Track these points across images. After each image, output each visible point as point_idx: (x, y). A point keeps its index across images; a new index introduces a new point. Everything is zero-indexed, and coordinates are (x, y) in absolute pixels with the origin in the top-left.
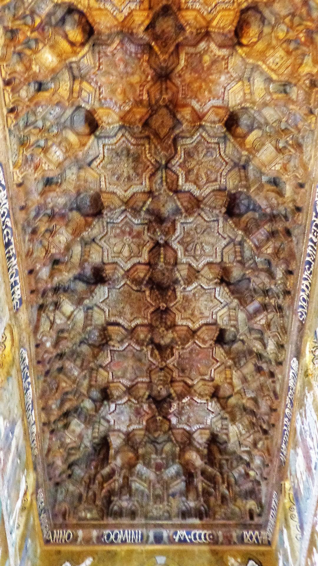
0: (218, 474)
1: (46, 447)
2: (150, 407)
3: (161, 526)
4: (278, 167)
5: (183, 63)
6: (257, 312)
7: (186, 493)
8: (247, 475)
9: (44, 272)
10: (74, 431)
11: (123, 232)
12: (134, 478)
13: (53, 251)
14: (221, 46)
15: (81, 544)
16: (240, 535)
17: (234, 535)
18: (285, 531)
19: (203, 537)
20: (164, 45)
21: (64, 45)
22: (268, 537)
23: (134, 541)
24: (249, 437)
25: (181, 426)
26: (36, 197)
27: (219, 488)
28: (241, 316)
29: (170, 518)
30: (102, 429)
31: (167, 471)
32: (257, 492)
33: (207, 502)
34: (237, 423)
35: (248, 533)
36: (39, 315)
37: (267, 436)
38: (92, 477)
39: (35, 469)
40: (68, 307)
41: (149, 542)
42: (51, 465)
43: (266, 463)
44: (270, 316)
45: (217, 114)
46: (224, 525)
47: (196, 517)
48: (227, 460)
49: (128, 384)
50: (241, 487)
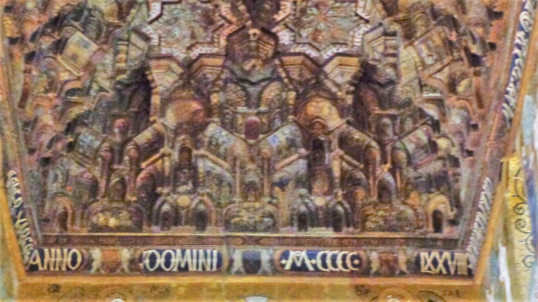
0: (374, 144)
1: (19, 87)
2: (234, 9)
3: (257, 241)
8: (433, 147)
10: (74, 57)
12: (202, 152)
15: (98, 274)
16: (413, 260)
17: (402, 258)
18: (503, 250)
19: (339, 262)
22: (468, 263)
23: (204, 268)
24: (440, 71)
25: (299, 49)
27: (374, 170)
29: (274, 227)
30: (134, 53)
31: (270, 138)
32: (451, 179)
33: (350, 197)
34: (416, 43)
35: (430, 254)
37: (477, 68)
38: (116, 148)
41: (234, 270)
43: (472, 123)
46: (382, 241)
47: (327, 226)
48: (393, 117)
50: (420, 171)
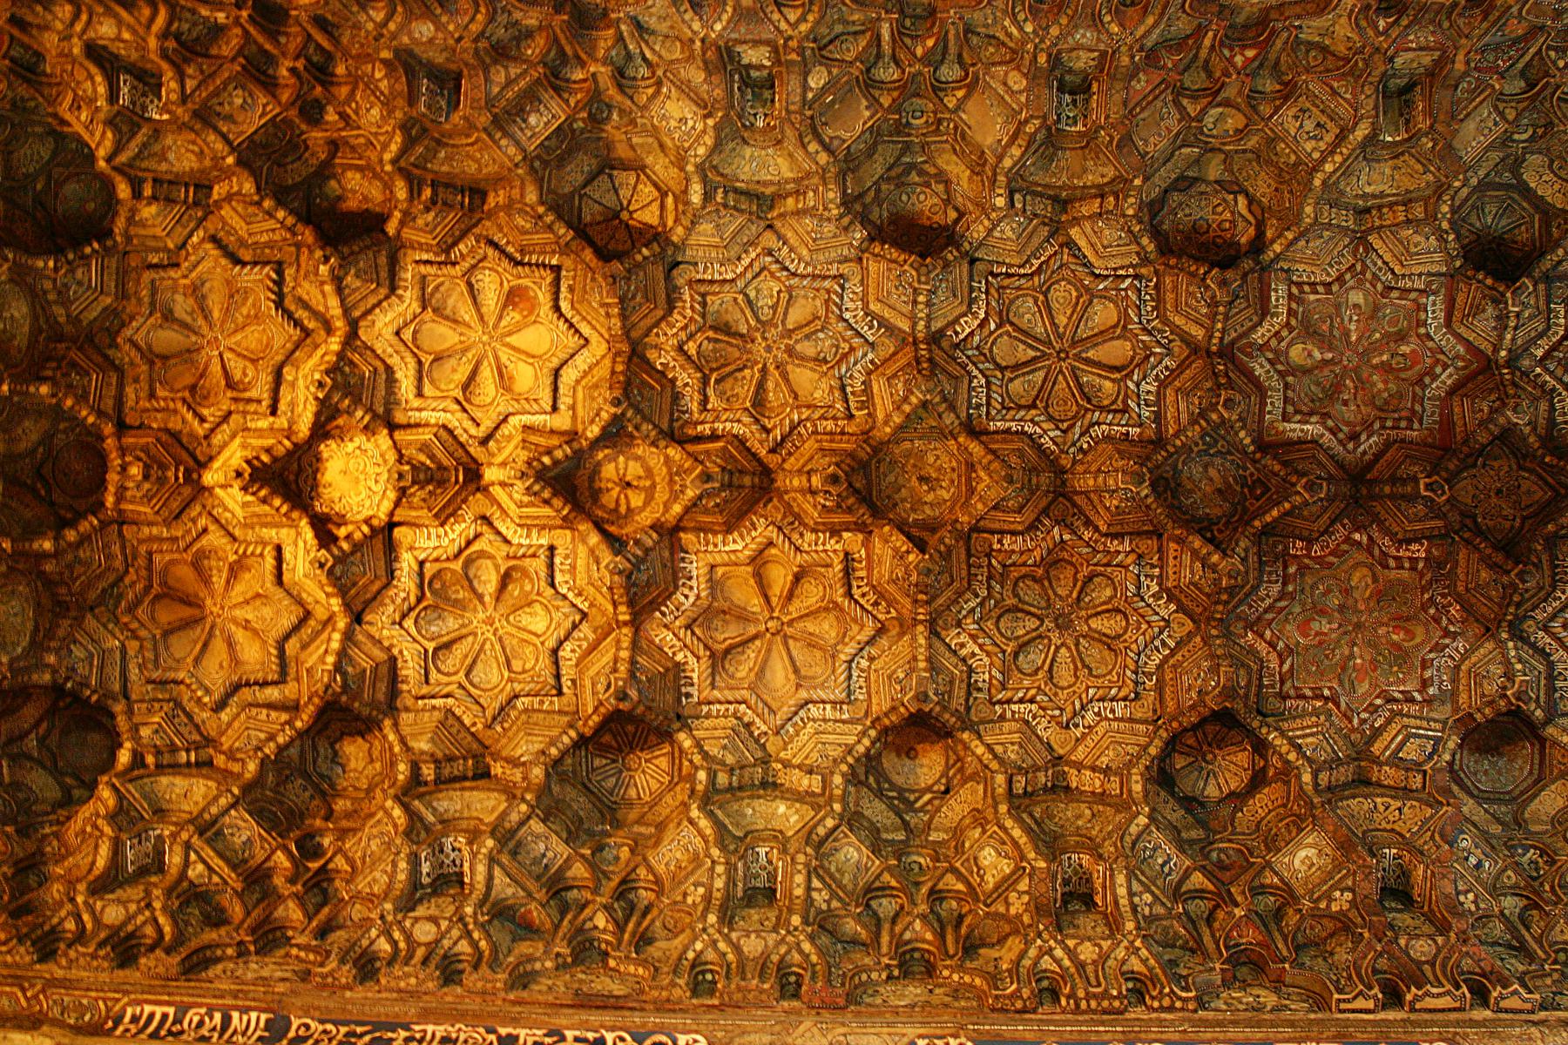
5: (1312, 428)
14: (1265, 311)
21: (1262, 803)
45: (1477, 310)
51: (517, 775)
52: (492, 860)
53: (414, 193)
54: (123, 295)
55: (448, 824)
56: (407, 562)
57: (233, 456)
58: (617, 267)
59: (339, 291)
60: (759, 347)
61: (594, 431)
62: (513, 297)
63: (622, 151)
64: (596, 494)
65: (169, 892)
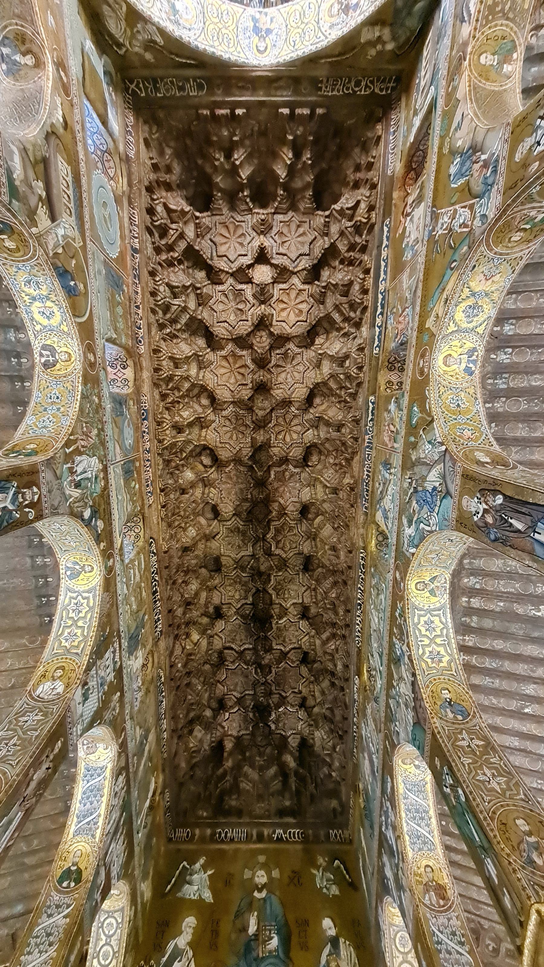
1: (174, 751)
2: (254, 715)
4: (335, 540)
5: (273, 476)
6: (328, 640)
7: (281, 793)
9: (179, 612)
11: (236, 582)
13: (186, 596)
20: (261, 467)
21: (201, 467)
26: (176, 560)
28: (318, 642)
29: (269, 817)
30: (218, 734)
36: (174, 643)
39: (163, 770)
40: (195, 636)
42: (176, 767)
44: (337, 643)
49: (239, 696)
51: (199, 312)
52: (179, 305)
53: (324, 287)
54: (304, 214)
55: (187, 295)
56: (244, 286)
57: (267, 242)
58: (306, 334)
59: (303, 270)
60: (289, 366)
61: (272, 330)
62: (301, 311)
63: (330, 335)
64: (259, 330)
65: (165, 224)
